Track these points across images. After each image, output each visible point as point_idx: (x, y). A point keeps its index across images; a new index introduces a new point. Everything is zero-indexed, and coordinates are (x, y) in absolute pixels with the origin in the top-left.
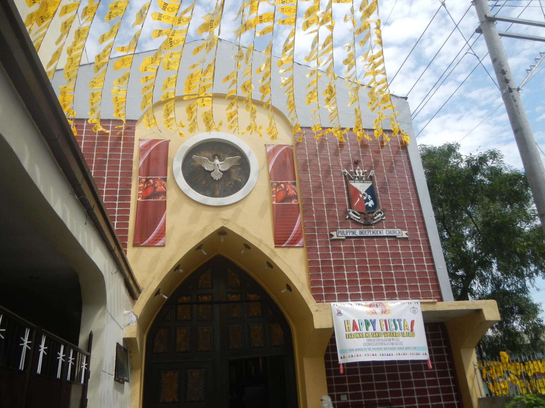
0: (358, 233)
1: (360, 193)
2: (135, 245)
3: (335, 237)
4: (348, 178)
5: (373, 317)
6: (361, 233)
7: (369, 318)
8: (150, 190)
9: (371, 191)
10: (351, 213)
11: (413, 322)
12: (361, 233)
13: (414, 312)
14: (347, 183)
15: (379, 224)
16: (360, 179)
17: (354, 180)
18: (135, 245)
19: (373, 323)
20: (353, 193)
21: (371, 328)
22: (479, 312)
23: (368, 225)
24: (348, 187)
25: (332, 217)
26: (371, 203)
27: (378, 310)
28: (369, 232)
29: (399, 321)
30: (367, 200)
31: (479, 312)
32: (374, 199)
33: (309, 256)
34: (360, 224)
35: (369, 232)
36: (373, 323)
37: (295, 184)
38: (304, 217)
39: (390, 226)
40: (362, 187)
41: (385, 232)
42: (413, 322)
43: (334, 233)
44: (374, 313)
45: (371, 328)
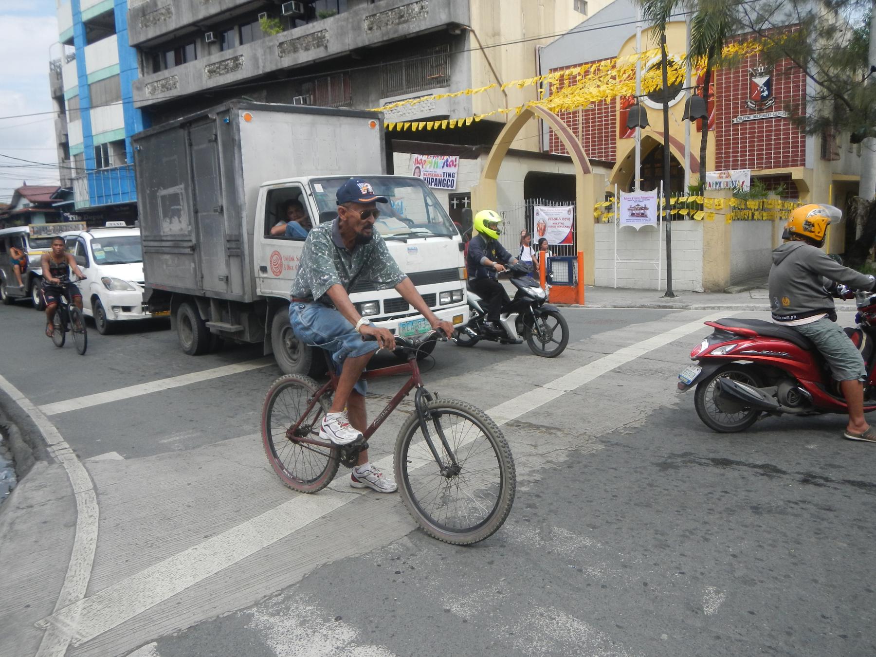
0: (752, 117)
1: (758, 86)
2: (621, 137)
3: (735, 122)
4: (752, 75)
5: (720, 180)
6: (754, 117)
7: (719, 180)
8: (627, 104)
9: (768, 84)
10: (749, 103)
11: (743, 182)
12: (754, 117)
13: (746, 176)
14: (750, 79)
15: (770, 109)
16: (761, 75)
17: (756, 76)
18: (621, 137)
19: (720, 183)
20: (754, 86)
21: (718, 186)
22: (789, 175)
23: (761, 110)
24: (752, 82)
25: (736, 108)
26: (765, 93)
27: (724, 176)
28: (760, 116)
29: (735, 181)
30: (763, 91)
31: (789, 175)
32: (768, 89)
33: (717, 137)
34: (754, 110)
35: (760, 116)
36: (720, 183)
37: (713, 85)
38: (717, 110)
39: (778, 109)
40: (760, 81)
41: (772, 115)
42: (743, 182)
43: (735, 120)
44: (722, 177)
45: (718, 186)
